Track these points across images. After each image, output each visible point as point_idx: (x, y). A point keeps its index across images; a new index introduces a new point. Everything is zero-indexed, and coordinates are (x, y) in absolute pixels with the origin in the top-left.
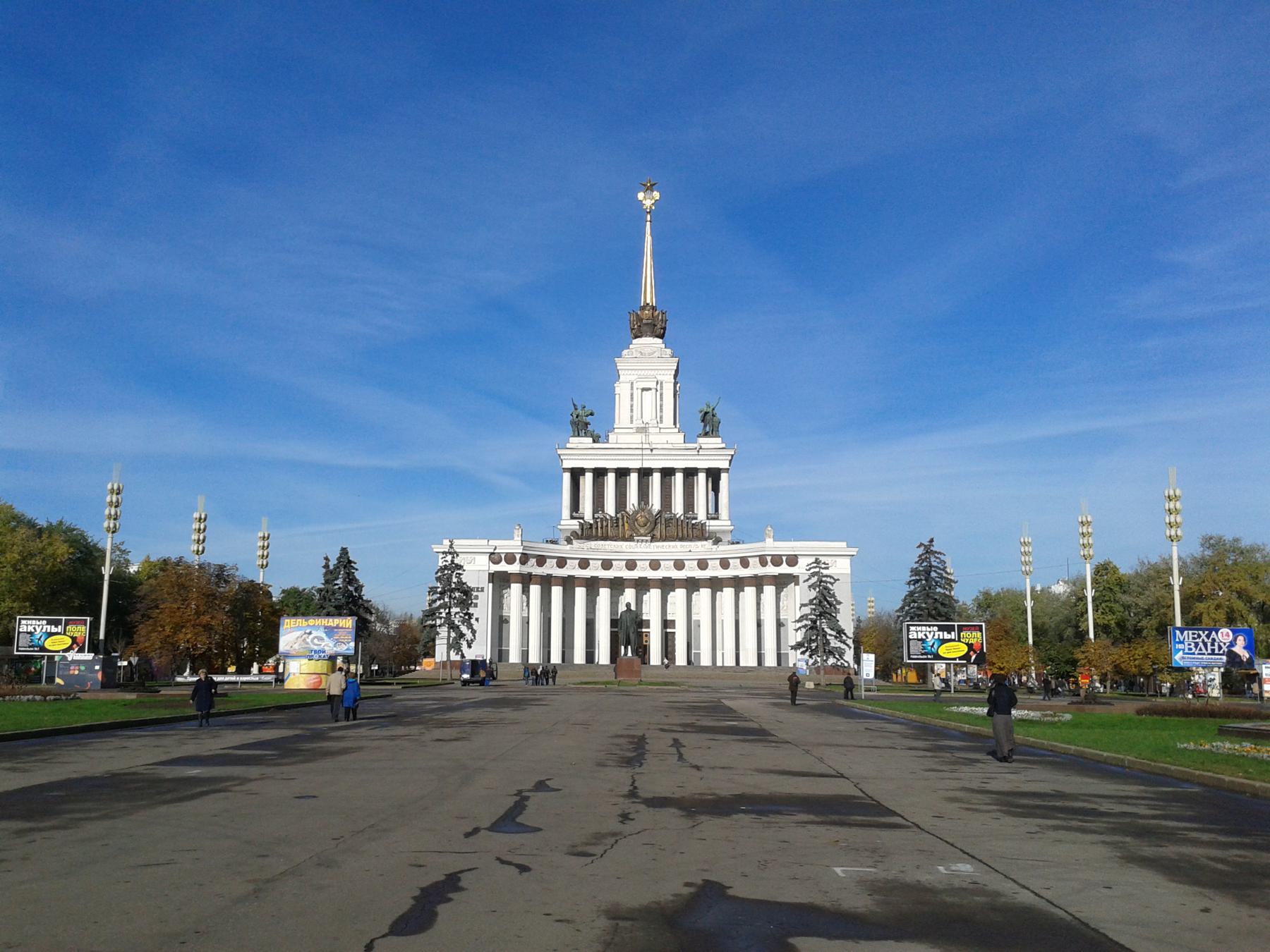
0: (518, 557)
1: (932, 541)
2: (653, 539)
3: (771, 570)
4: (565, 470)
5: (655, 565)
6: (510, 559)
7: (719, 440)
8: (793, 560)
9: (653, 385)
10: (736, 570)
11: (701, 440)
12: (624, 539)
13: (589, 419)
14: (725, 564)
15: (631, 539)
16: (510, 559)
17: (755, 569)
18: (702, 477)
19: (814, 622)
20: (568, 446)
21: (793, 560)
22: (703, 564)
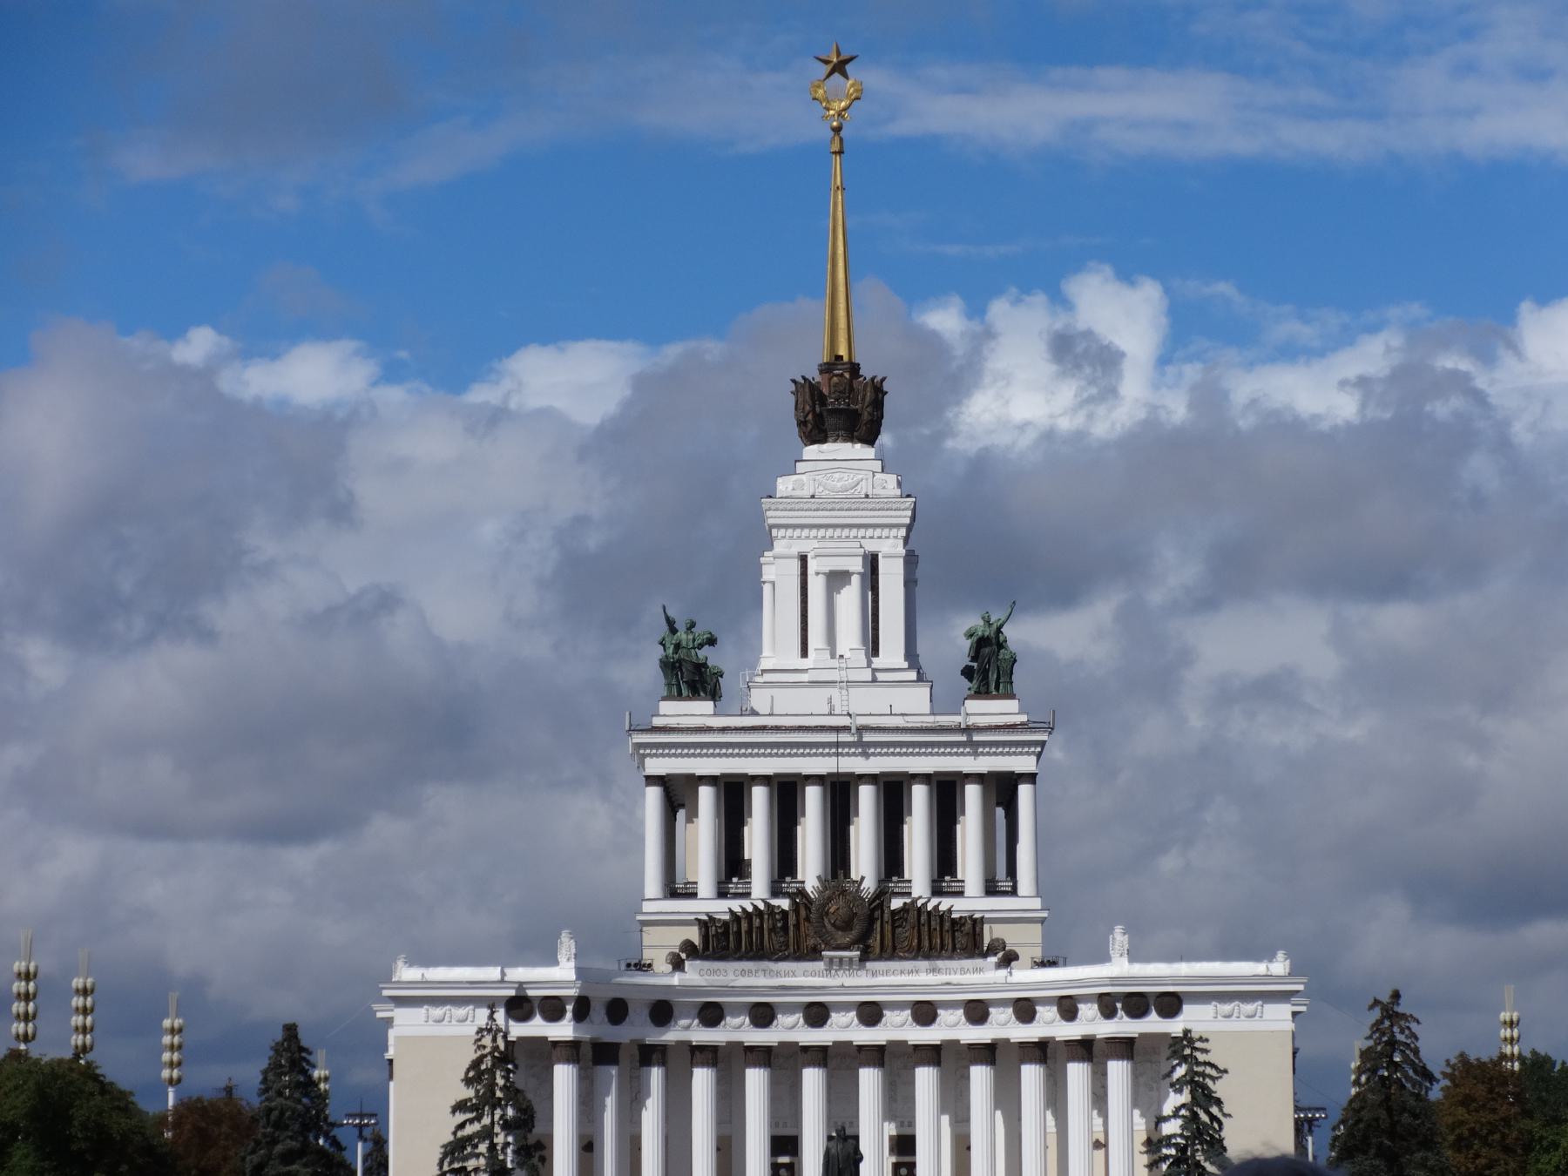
0: (569, 1008)
1: (1396, 996)
2: (865, 957)
3: (1123, 1026)
4: (652, 780)
5: (871, 1014)
6: (553, 1009)
7: (1012, 705)
8: (1170, 1004)
9: (856, 565)
10: (1048, 1025)
11: (973, 706)
12: (799, 956)
13: (703, 653)
14: (1025, 1010)
15: (814, 954)
16: (553, 1009)
17: (1089, 1023)
18: (972, 795)
19: (1182, 1149)
20: (657, 722)
21: (1170, 1004)
22: (977, 1012)
